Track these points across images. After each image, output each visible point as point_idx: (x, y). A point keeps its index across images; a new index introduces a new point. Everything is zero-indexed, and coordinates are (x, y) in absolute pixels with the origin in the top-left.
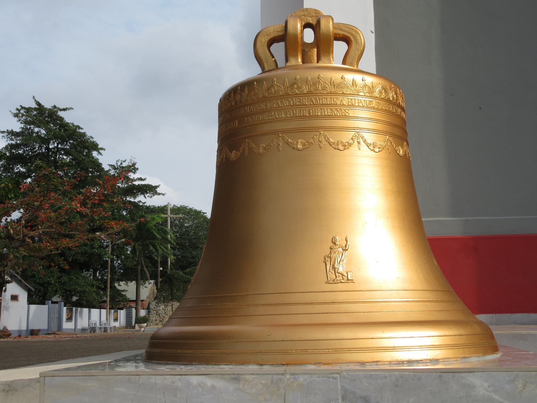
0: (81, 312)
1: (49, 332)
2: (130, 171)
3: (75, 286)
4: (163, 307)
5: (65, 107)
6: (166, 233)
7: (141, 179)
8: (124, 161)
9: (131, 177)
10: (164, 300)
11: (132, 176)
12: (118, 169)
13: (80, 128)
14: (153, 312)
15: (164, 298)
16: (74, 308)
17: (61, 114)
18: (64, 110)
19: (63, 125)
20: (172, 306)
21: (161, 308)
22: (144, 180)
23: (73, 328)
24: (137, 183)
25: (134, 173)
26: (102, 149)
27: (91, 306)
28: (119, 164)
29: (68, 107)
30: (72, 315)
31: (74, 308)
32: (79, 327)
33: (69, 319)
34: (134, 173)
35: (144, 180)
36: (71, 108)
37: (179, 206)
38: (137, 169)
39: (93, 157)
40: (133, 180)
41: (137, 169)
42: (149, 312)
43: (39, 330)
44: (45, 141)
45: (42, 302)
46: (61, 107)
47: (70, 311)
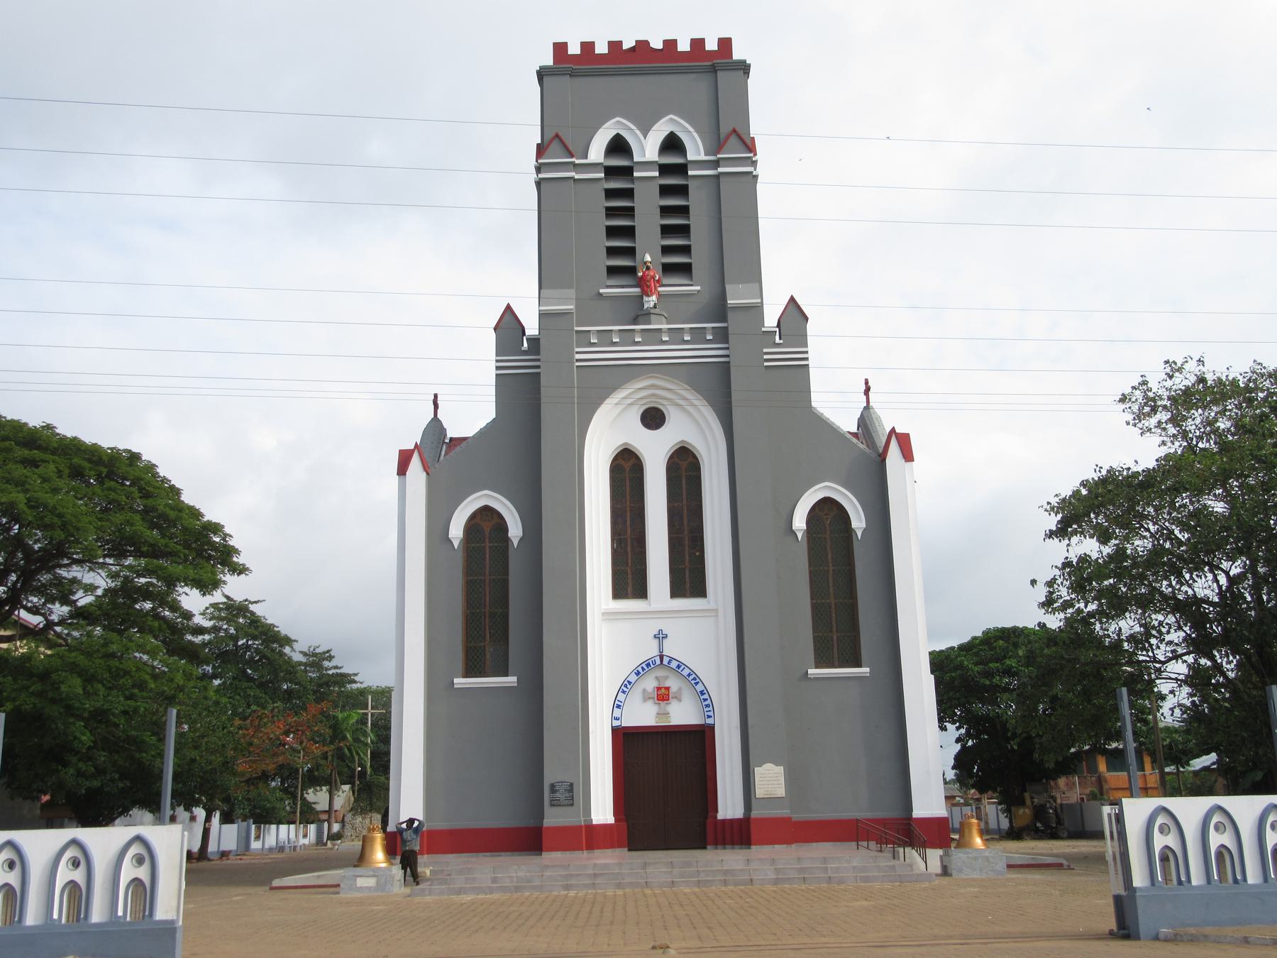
0: (269, 829)
1: (238, 853)
2: (324, 659)
3: (264, 801)
4: (360, 819)
5: (256, 600)
6: (365, 734)
7: (336, 667)
8: (317, 647)
9: (326, 666)
10: (361, 811)
11: (326, 664)
12: (309, 655)
13: (275, 626)
14: (348, 827)
15: (362, 809)
16: (262, 825)
17: (252, 607)
18: (256, 602)
19: (255, 621)
20: (371, 818)
21: (358, 821)
22: (341, 668)
23: (261, 847)
24: (330, 672)
25: (330, 661)
26: (296, 641)
27: (279, 822)
28: (312, 650)
29: (261, 599)
30: (260, 833)
31: (262, 825)
32: (267, 846)
33: (258, 838)
34: (330, 661)
35: (341, 668)
36: (264, 600)
37: (383, 687)
38: (334, 657)
39: (285, 654)
40: (327, 669)
41: (334, 657)
42: (343, 826)
43: (230, 852)
44: (235, 639)
45: (232, 822)
46: (252, 600)
47: (258, 829)
